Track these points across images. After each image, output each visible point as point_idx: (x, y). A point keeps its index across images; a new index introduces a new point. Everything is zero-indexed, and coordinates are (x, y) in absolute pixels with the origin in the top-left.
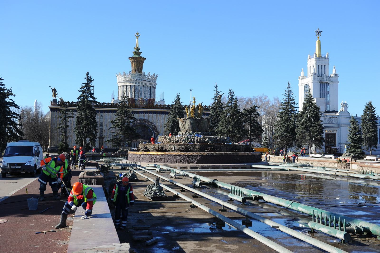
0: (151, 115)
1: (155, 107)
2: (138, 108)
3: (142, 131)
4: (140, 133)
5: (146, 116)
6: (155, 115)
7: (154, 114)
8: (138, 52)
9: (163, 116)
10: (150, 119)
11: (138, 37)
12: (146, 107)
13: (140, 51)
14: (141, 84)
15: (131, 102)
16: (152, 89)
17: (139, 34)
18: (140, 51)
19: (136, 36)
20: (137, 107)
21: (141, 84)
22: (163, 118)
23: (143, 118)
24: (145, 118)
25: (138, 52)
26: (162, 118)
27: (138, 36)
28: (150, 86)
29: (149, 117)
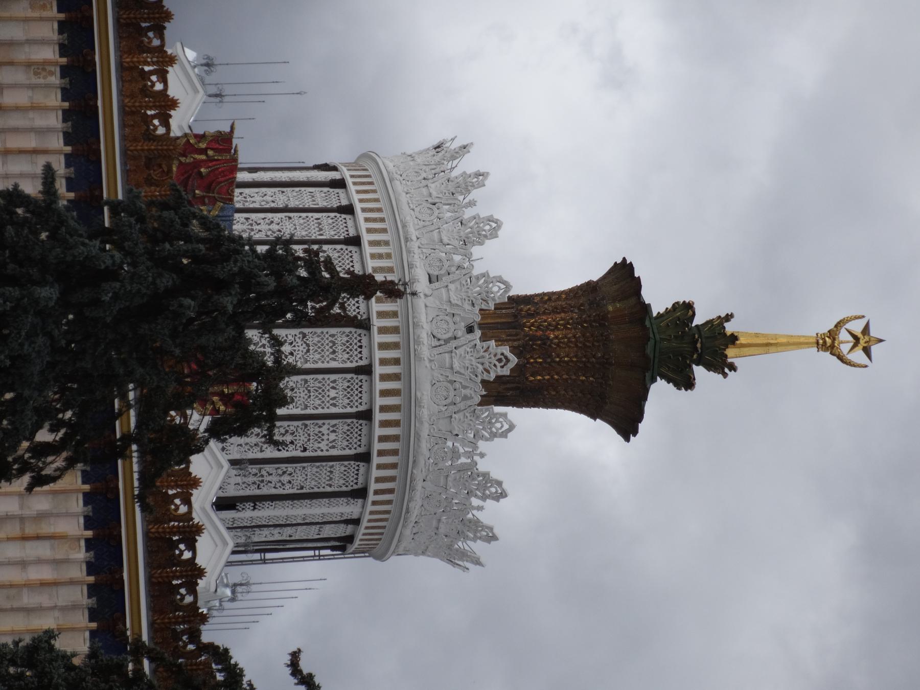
8: (693, 346)
11: (828, 343)
14: (383, 346)
15: (197, 164)
16: (339, 477)
17: (858, 356)
19: (839, 325)
21: (383, 346)
22: (41, 516)
25: (693, 346)
27: (845, 348)
28: (365, 457)
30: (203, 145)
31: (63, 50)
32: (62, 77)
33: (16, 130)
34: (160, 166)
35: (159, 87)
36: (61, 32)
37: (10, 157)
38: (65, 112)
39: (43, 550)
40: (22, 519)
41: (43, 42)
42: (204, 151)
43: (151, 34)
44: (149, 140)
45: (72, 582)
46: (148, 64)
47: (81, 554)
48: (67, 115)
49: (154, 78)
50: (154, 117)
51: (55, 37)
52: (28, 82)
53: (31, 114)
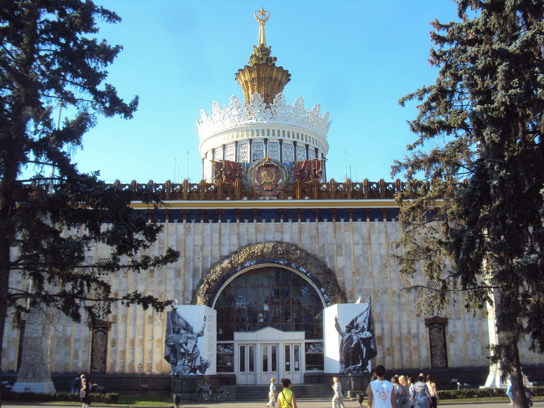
0: (308, 224)
1: (327, 191)
2: (256, 199)
3: (277, 293)
4: (266, 302)
5: (289, 232)
6: (326, 226)
7: (321, 220)
9: (363, 226)
10: (307, 244)
12: (287, 192)
13: (272, 55)
15: (226, 175)
18: (272, 55)
20: (252, 196)
22: (362, 237)
23: (278, 239)
24: (287, 238)
26: (357, 237)
29: (306, 236)
30: (219, 172)
31: (180, 221)
32: (191, 222)
33: (211, 240)
34: (227, 188)
35: (196, 187)
36: (173, 222)
37: (222, 243)
38: (204, 222)
39: (374, 237)
40: (363, 244)
41: (176, 228)
42: (221, 172)
43: (175, 189)
44: (217, 191)
45: (386, 227)
46: (187, 190)
47: (376, 223)
48: (206, 221)
49: (192, 189)
50: (207, 189)
51: (175, 224)
52: (192, 235)
53: (205, 235)
